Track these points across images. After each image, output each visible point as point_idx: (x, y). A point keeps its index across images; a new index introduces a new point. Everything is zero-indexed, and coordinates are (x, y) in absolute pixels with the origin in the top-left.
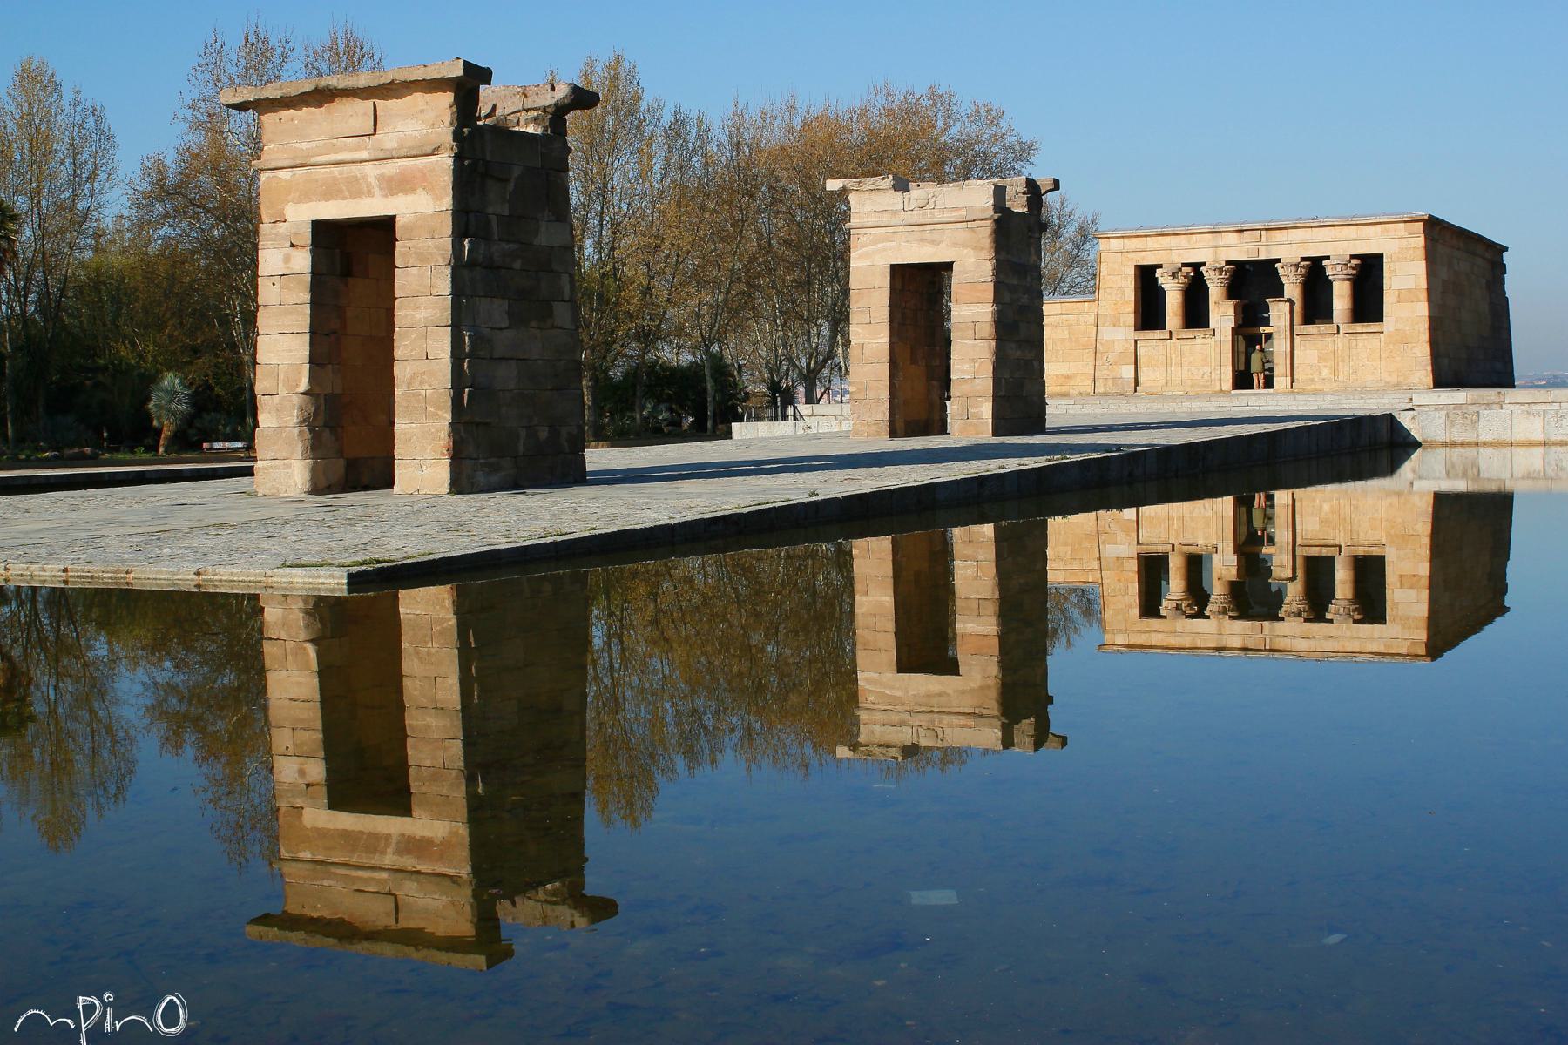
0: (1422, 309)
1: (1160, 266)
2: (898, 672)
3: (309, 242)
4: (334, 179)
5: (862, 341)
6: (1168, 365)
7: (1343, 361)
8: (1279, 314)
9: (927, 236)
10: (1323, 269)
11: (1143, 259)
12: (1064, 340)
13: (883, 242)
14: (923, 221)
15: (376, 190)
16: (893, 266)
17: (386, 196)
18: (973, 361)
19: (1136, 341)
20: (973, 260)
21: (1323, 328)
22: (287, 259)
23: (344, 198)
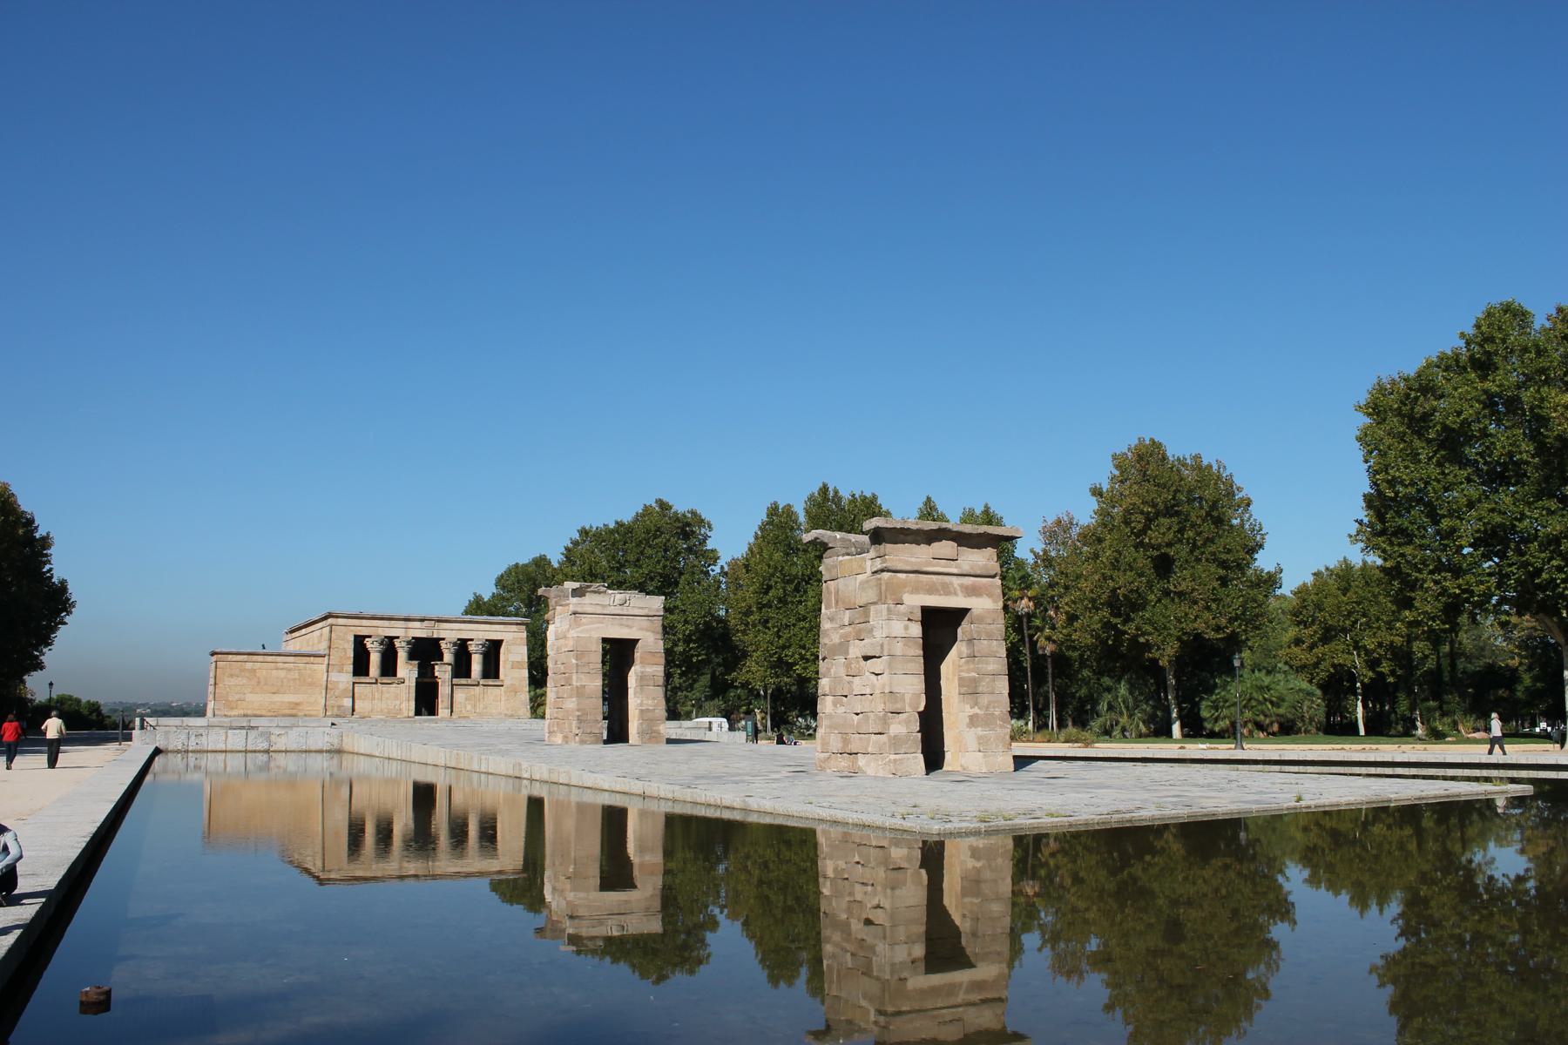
0: (525, 673)
1: (370, 637)
2: (601, 891)
3: (920, 619)
4: (933, 582)
5: (584, 684)
6: (373, 699)
7: (479, 700)
8: (443, 672)
9: (624, 622)
10: (467, 647)
11: (360, 631)
12: (295, 679)
13: (599, 623)
14: (622, 613)
15: (959, 592)
16: (603, 639)
17: (965, 597)
18: (654, 699)
19: (354, 683)
20: (652, 639)
21: (469, 681)
22: (906, 628)
23: (940, 595)
